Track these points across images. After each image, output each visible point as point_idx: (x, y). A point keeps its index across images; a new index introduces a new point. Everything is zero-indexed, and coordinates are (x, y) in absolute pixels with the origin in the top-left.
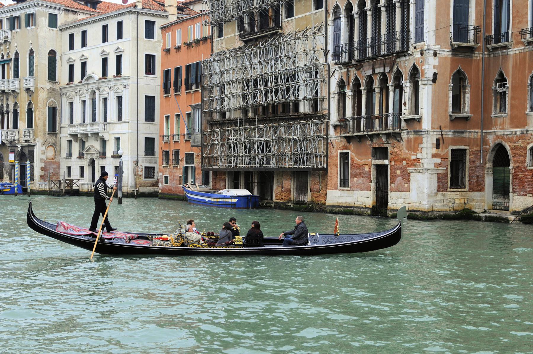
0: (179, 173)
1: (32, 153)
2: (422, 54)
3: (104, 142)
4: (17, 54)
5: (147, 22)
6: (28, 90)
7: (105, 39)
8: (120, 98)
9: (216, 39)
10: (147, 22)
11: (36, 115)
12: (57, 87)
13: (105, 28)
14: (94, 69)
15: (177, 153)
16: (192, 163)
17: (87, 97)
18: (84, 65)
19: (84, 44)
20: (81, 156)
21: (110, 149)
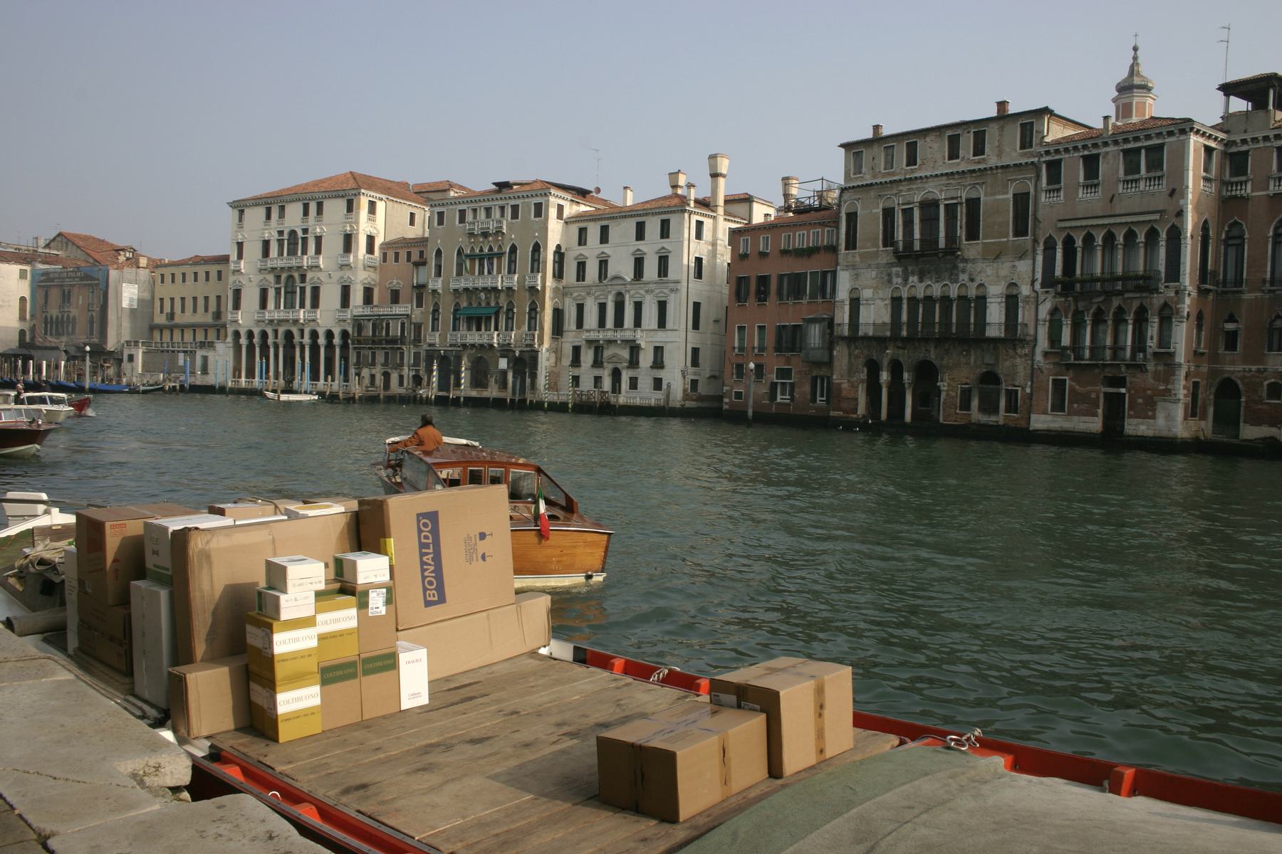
0: (764, 390)
2: (1177, 293)
4: (513, 249)
14: (622, 267)
20: (597, 363)
21: (646, 359)
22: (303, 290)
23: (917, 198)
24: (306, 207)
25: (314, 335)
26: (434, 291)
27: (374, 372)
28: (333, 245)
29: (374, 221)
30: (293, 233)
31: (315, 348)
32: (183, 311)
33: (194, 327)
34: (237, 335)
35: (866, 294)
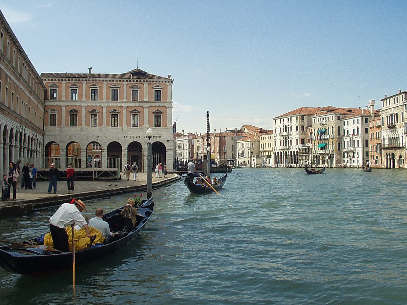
1: (333, 156)
3: (354, 153)
4: (328, 128)
5: (365, 119)
6: (332, 138)
7: (354, 124)
8: (358, 141)
9: (382, 127)
10: (365, 119)
11: (334, 145)
12: (340, 137)
13: (354, 120)
14: (351, 132)
15: (374, 156)
16: (377, 158)
17: (349, 140)
18: (348, 131)
19: (348, 125)
20: (347, 157)
21: (356, 155)
22: (288, 140)
23: (390, 114)
24: (288, 119)
25: (291, 152)
26: (314, 140)
27: (303, 161)
28: (294, 129)
29: (303, 121)
30: (286, 126)
31: (291, 155)
32: (266, 147)
33: (268, 151)
34: (275, 153)
35: (385, 137)
